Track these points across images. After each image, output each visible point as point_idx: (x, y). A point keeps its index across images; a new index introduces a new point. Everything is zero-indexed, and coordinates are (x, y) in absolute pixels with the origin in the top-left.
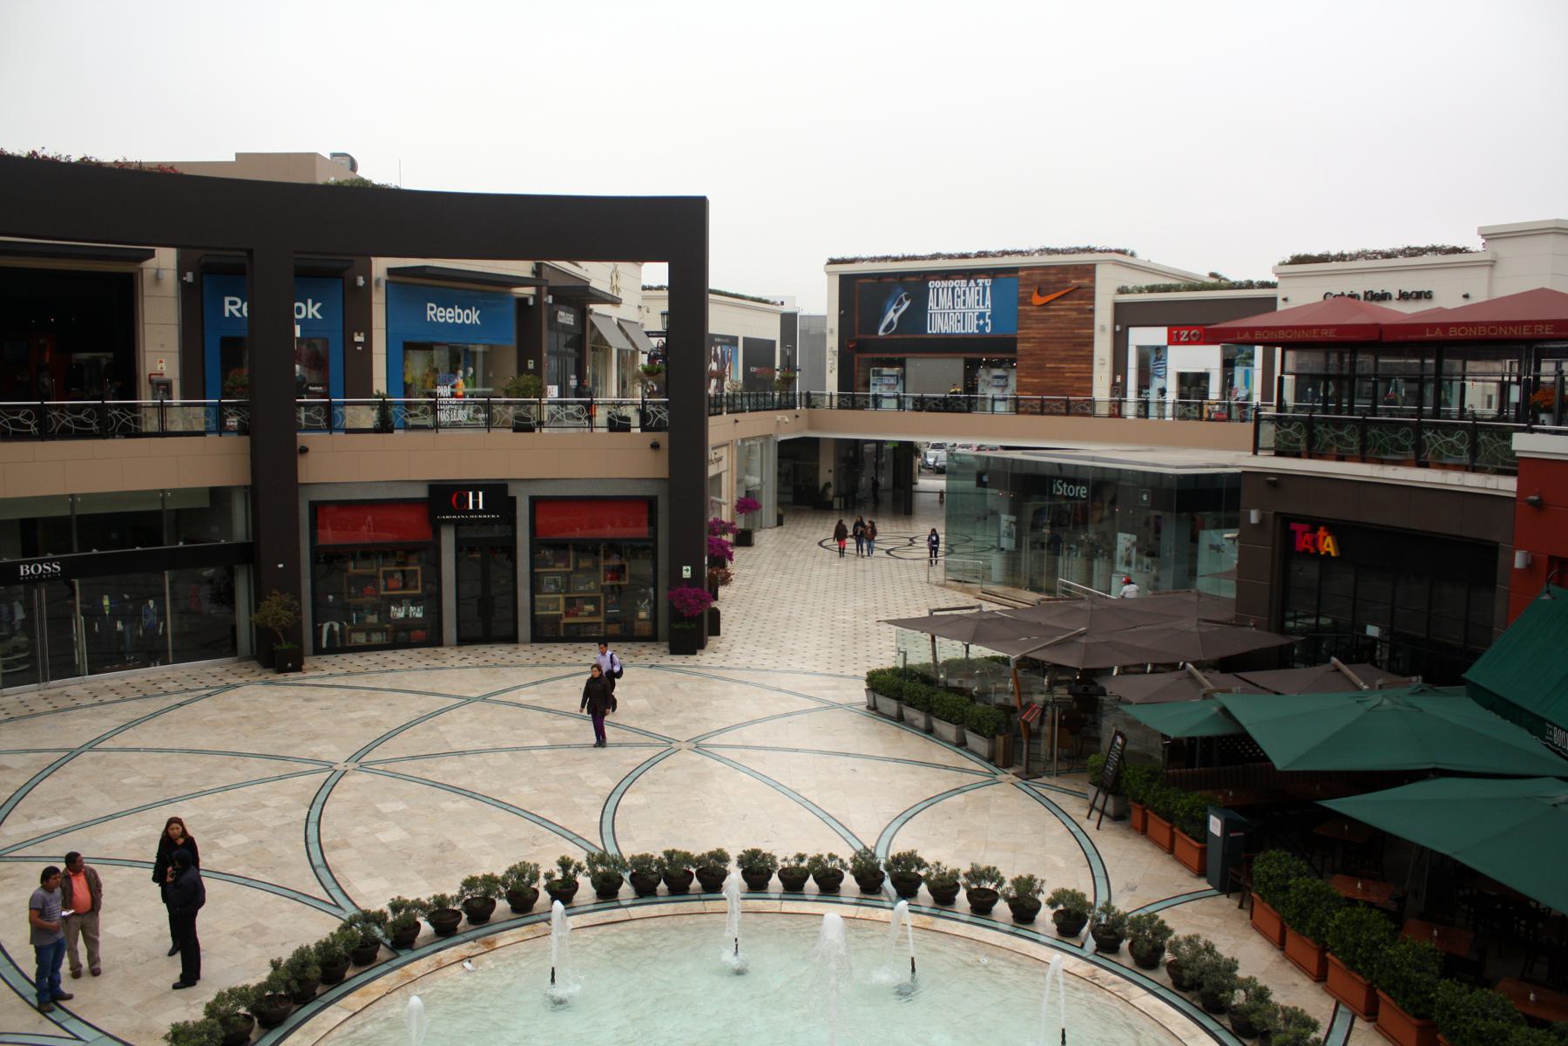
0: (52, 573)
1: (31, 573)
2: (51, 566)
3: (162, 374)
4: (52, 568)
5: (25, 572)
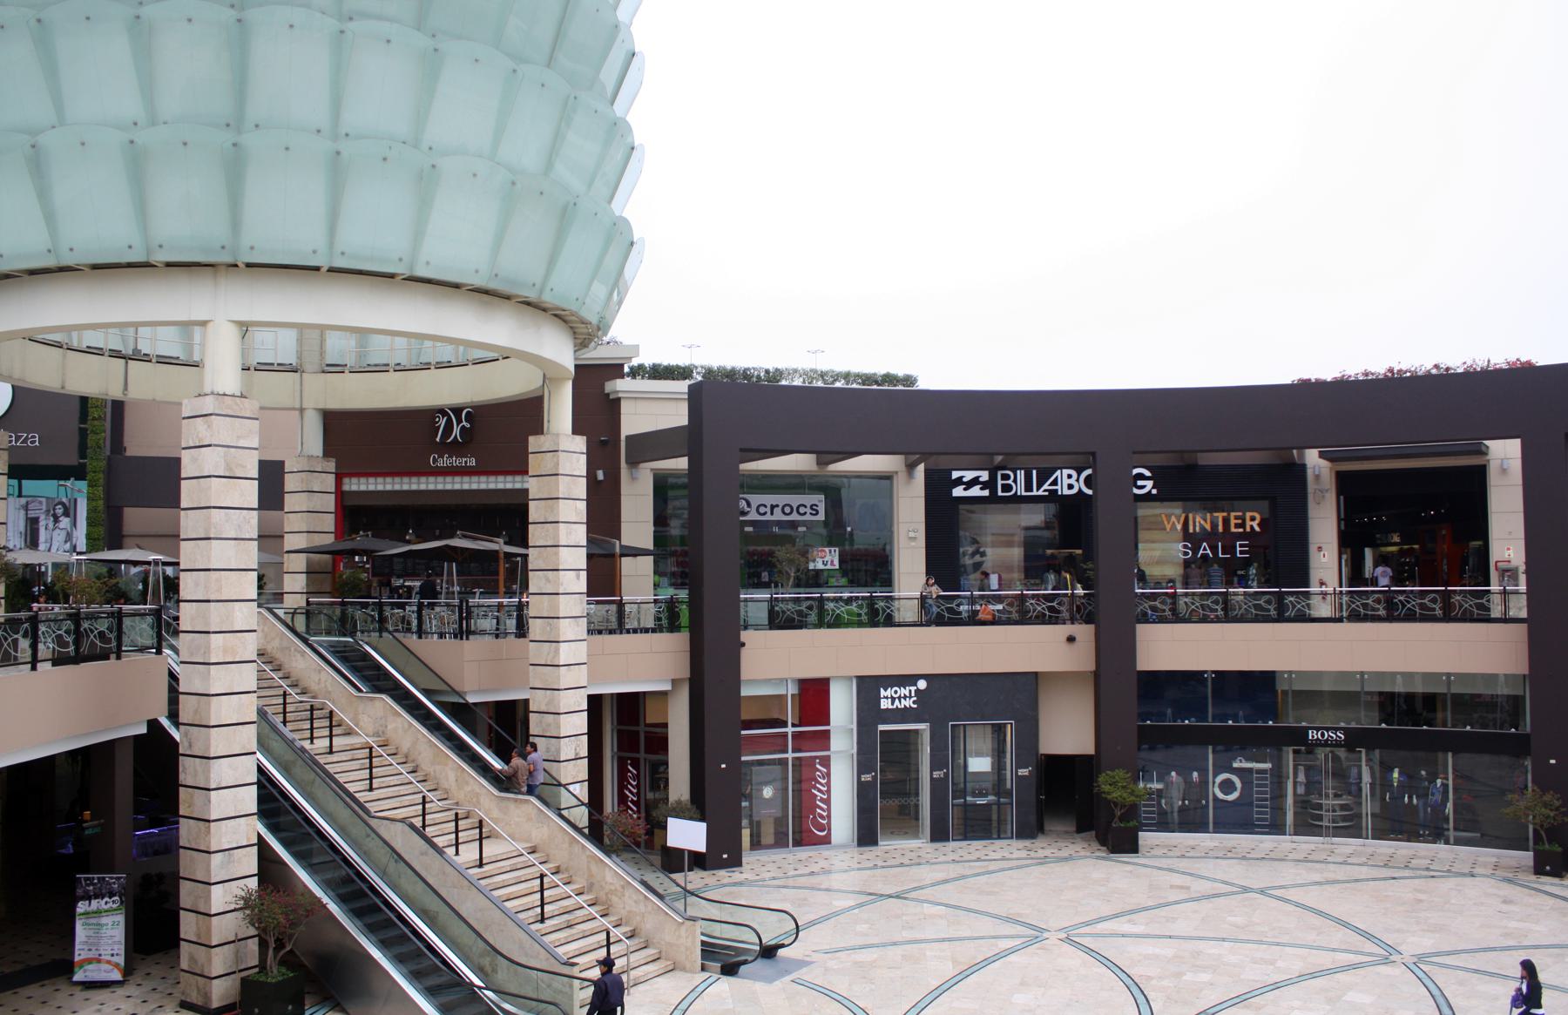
0: (1336, 740)
1: (1318, 739)
2: (1336, 734)
3: (1509, 561)
4: (1337, 736)
5: (1313, 736)
